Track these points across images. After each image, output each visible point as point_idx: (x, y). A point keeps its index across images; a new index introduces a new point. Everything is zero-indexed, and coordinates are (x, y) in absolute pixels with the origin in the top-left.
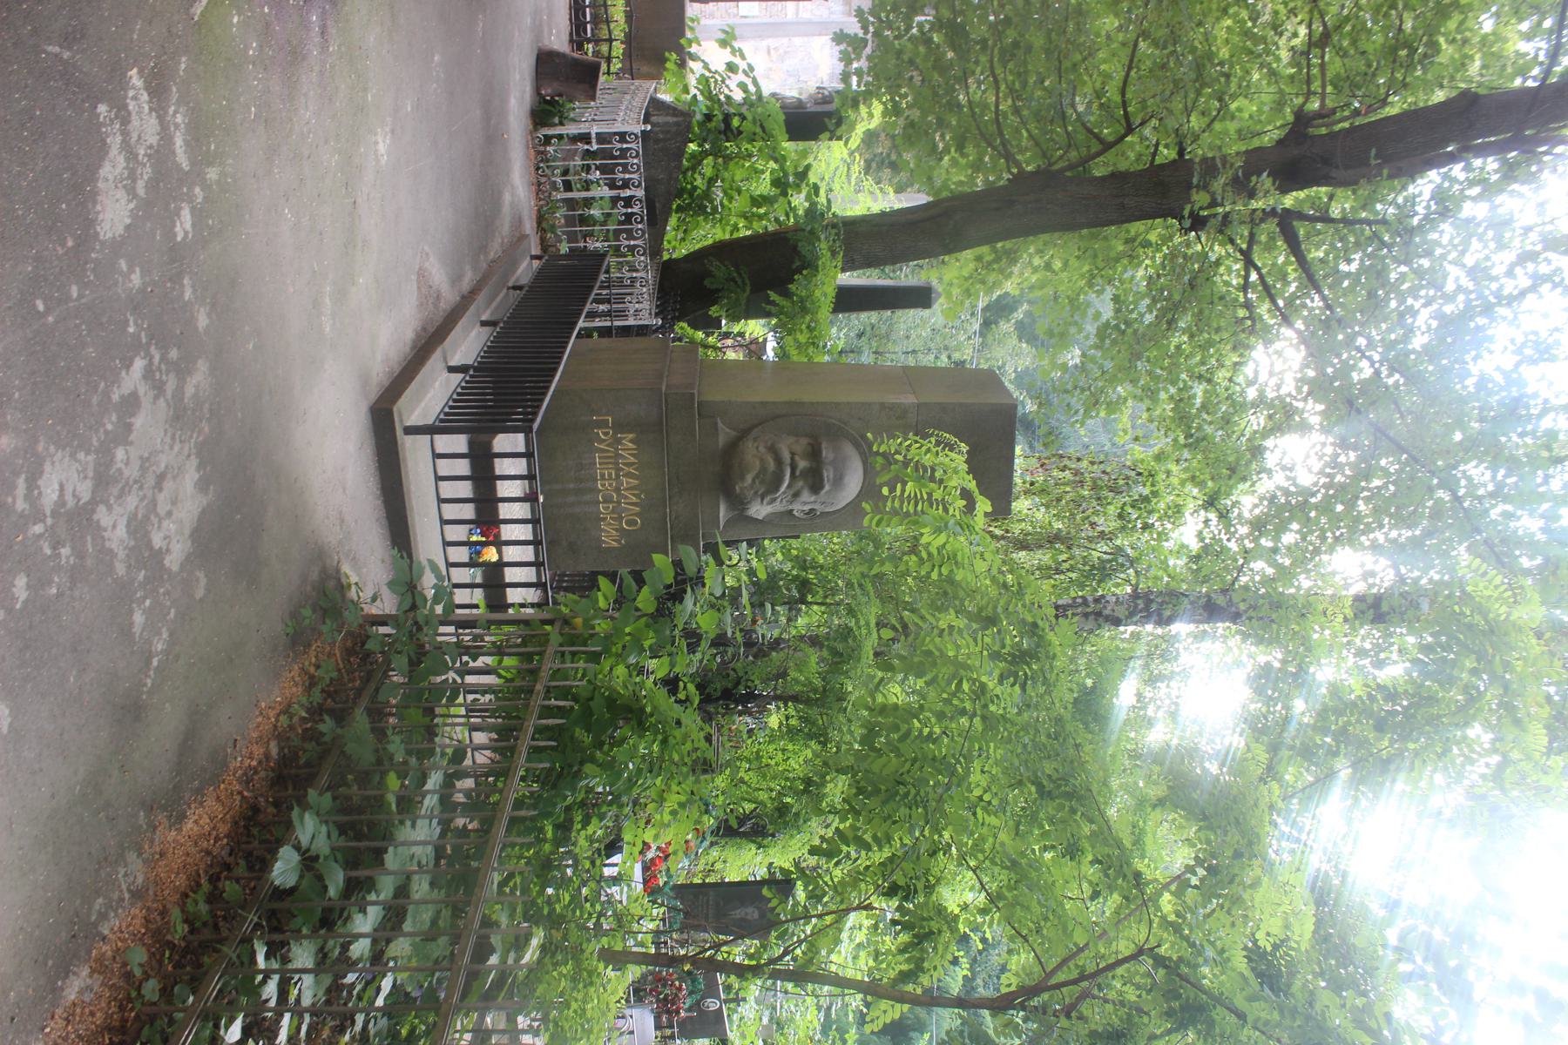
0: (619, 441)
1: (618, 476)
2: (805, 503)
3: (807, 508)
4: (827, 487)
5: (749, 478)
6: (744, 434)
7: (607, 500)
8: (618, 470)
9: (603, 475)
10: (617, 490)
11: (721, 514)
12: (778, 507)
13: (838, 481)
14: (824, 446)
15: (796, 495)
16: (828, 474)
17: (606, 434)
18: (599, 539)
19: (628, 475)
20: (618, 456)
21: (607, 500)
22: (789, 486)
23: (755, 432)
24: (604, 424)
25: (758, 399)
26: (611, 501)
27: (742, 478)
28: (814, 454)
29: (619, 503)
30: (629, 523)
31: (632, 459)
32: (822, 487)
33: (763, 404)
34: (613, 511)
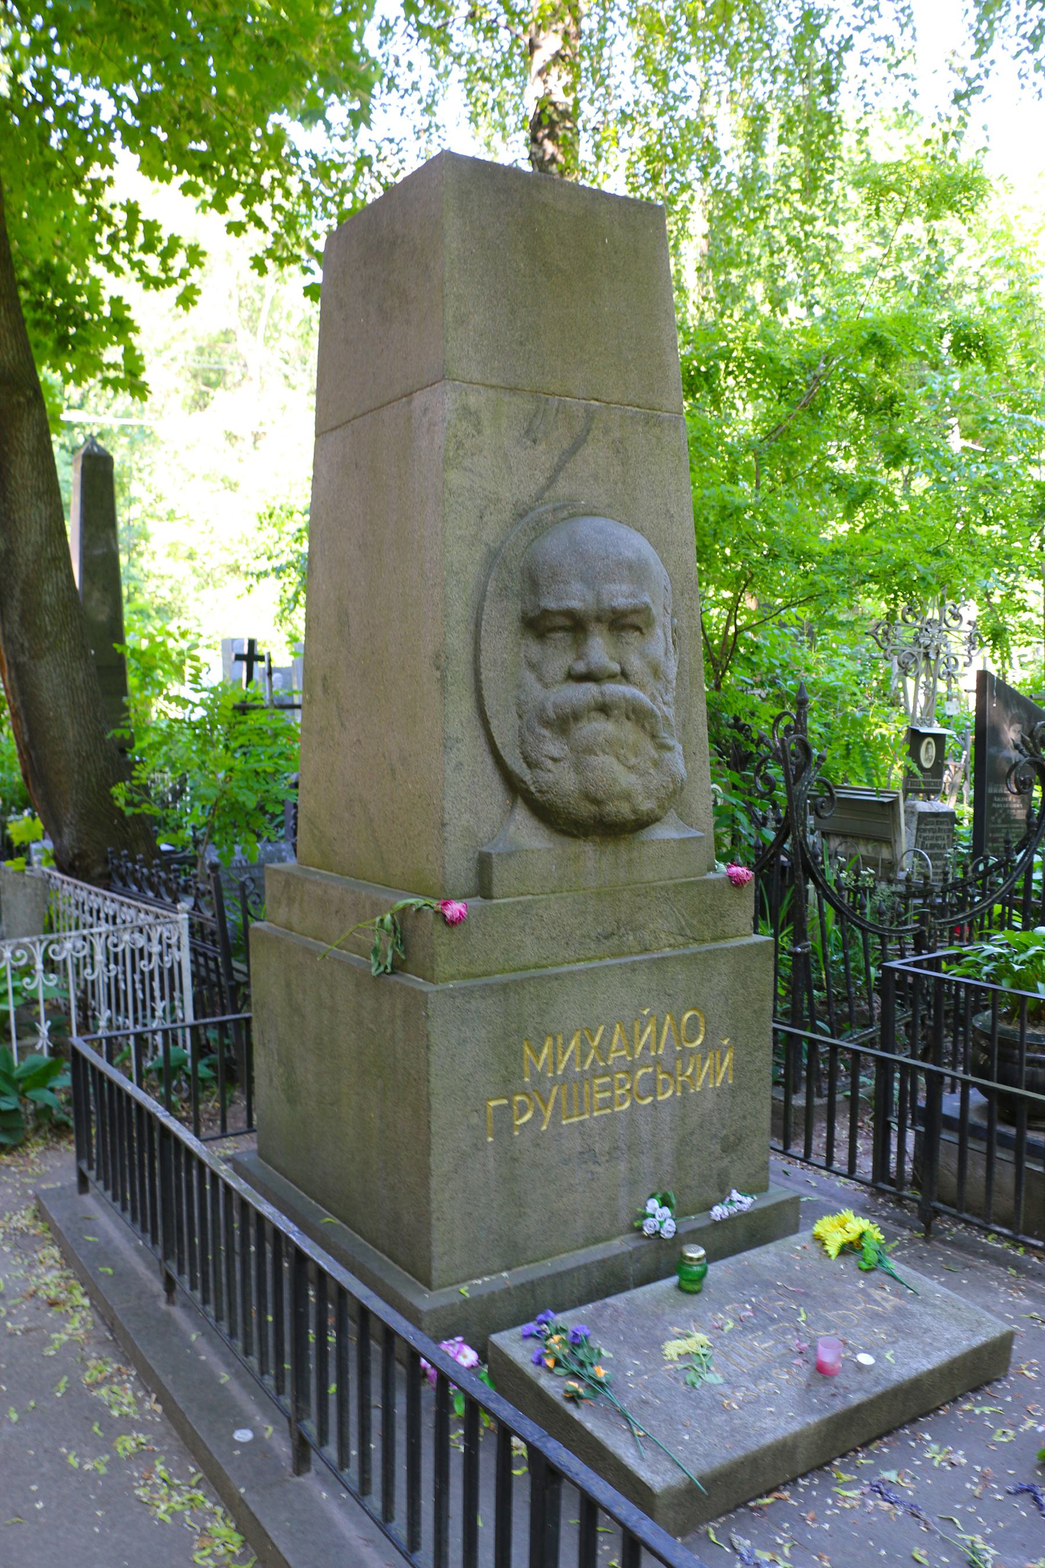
0: (539, 1078)
1: (607, 1072)
4: (647, 599)
5: (627, 780)
9: (607, 1103)
11: (675, 835)
13: (637, 571)
15: (656, 672)
16: (620, 595)
18: (719, 1093)
19: (603, 1051)
22: (642, 687)
23: (517, 766)
26: (653, 1077)
27: (627, 797)
29: (657, 1061)
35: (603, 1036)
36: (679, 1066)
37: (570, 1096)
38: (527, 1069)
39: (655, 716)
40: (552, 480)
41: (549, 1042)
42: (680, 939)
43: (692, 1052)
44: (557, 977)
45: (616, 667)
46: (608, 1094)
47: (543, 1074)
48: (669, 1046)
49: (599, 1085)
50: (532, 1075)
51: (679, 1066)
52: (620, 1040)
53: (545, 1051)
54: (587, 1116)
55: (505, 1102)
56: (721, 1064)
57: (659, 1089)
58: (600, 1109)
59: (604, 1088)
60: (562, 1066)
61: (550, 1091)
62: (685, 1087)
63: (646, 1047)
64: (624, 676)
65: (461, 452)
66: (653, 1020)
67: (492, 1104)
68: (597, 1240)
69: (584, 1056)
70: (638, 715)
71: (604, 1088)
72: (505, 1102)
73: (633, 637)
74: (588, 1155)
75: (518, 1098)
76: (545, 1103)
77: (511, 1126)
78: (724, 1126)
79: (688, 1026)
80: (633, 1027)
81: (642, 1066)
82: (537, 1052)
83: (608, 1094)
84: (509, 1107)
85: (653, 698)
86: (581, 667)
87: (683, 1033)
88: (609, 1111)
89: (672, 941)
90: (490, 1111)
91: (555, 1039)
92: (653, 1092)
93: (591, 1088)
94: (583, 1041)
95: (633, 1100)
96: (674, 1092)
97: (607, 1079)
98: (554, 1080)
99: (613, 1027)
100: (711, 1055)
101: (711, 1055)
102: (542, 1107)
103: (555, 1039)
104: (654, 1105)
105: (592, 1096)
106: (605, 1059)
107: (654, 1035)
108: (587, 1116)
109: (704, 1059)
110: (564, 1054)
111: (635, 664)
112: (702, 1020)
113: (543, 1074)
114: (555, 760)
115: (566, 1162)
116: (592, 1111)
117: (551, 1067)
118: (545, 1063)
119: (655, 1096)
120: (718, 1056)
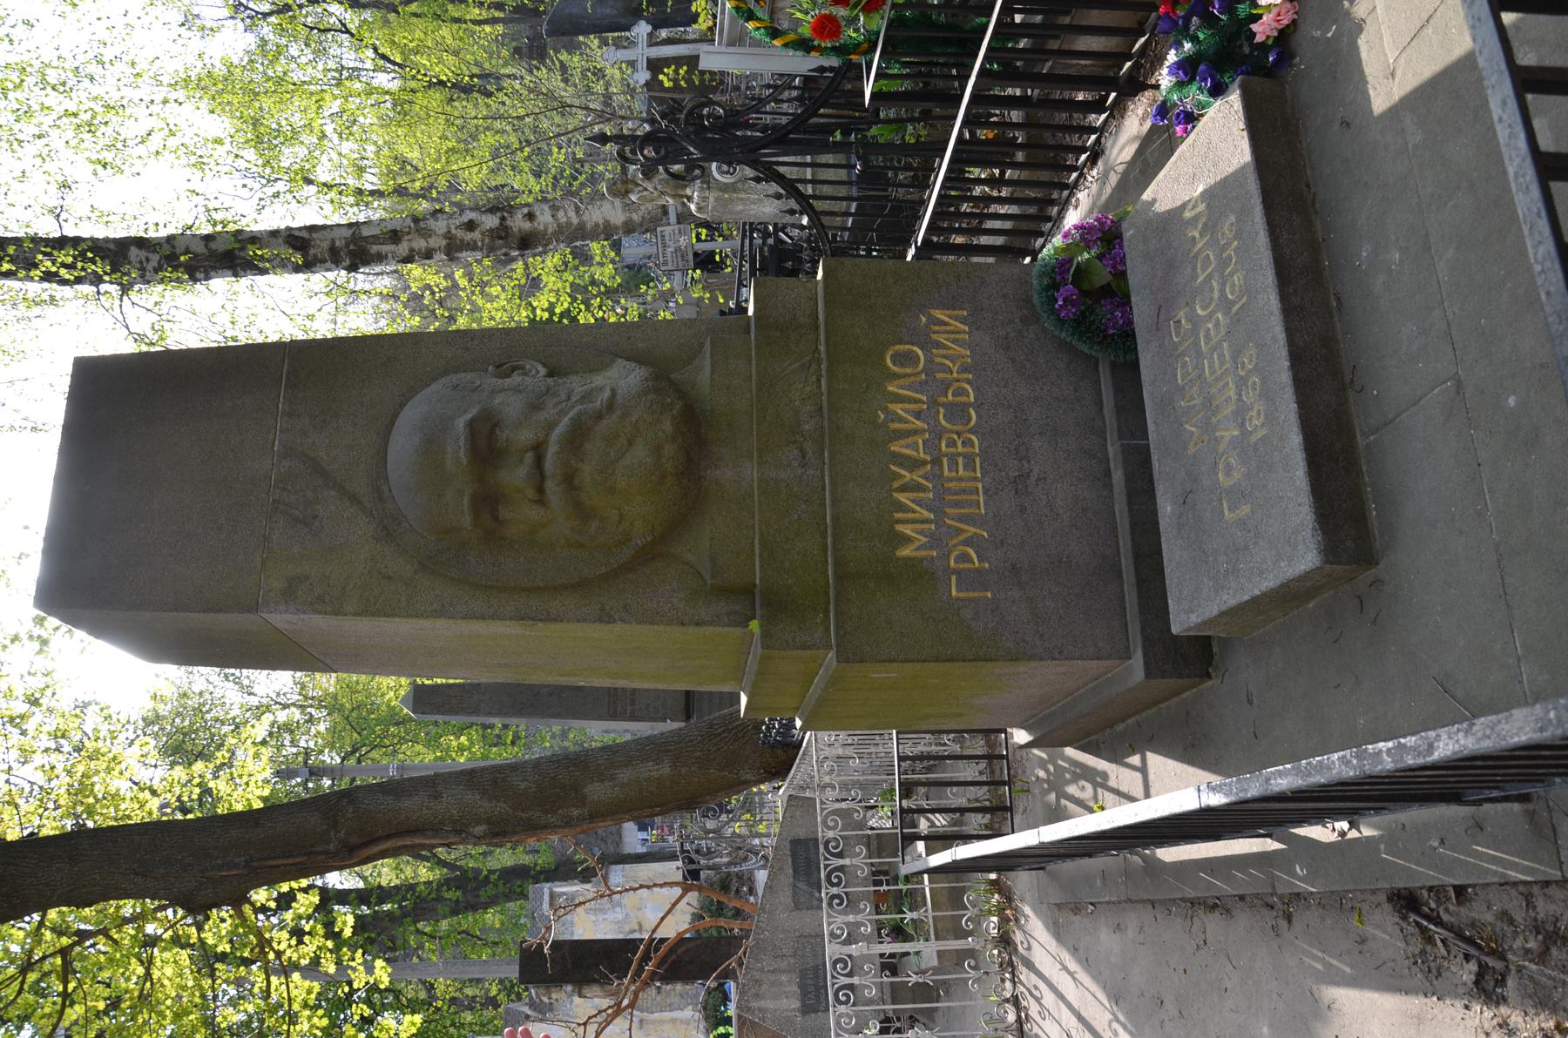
0: (935, 541)
1: (937, 462)
2: (517, 390)
3: (516, 379)
4: (461, 423)
6: (653, 553)
7: (957, 412)
8: (937, 477)
9: (970, 465)
10: (938, 433)
11: (707, 370)
12: (577, 385)
13: (431, 443)
14: (467, 521)
17: (965, 558)
19: (913, 464)
20: (939, 512)
21: (957, 412)
22: (551, 426)
24: (970, 579)
25: (618, 628)
27: (657, 451)
28: (488, 501)
29: (933, 403)
30: (906, 359)
31: (903, 498)
32: (471, 424)
33: (605, 617)
34: (946, 385)
35: (901, 465)
36: (940, 376)
37: (957, 504)
38: (923, 553)
39: (579, 414)
40: (354, 499)
41: (899, 528)
42: (814, 367)
43: (929, 361)
44: (835, 518)
45: (529, 457)
46: (960, 460)
47: (931, 536)
48: (920, 387)
49: (950, 470)
50: (931, 548)
51: (940, 376)
52: (907, 446)
53: (909, 532)
54: (980, 486)
55: (954, 578)
56: (946, 324)
57: (963, 399)
58: (974, 470)
59: (954, 465)
60: (926, 513)
61: (950, 527)
62: (964, 369)
63: (918, 415)
64: (538, 449)
65: (327, 598)
66: (892, 406)
67: (954, 592)
68: (1108, 473)
69: (919, 488)
70: (578, 436)
71: (954, 465)
72: (954, 578)
73: (503, 435)
74: (1020, 483)
75: (952, 563)
76: (960, 531)
77: (978, 570)
78: (1012, 321)
79: (902, 365)
80: (895, 431)
81: (937, 419)
82: (908, 540)
83: (960, 460)
84: (958, 572)
85: (564, 412)
86: (531, 493)
87: (908, 371)
88: (978, 460)
89: (814, 378)
90: (961, 595)
91: (899, 521)
92: (965, 407)
93: (951, 480)
94: (903, 489)
95: (970, 431)
96: (969, 382)
97: (945, 460)
98: (936, 522)
99: (894, 454)
100: (935, 337)
101: (935, 337)
102: (965, 536)
103: (899, 521)
104: (978, 406)
105: (961, 479)
106: (924, 463)
107: (906, 406)
108: (980, 486)
109: (938, 345)
110: (914, 511)
111: (526, 436)
112: (897, 347)
113: (931, 536)
114: (621, 517)
115: (1023, 509)
116: (975, 479)
117: (926, 526)
118: (921, 533)
119: (969, 405)
120: (937, 328)
